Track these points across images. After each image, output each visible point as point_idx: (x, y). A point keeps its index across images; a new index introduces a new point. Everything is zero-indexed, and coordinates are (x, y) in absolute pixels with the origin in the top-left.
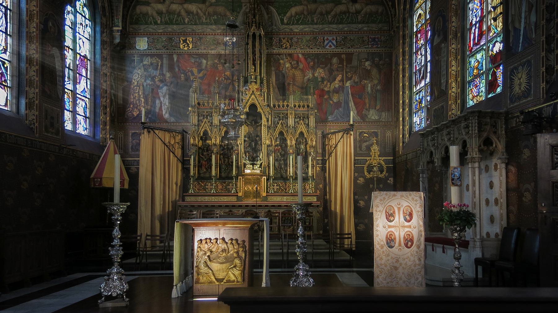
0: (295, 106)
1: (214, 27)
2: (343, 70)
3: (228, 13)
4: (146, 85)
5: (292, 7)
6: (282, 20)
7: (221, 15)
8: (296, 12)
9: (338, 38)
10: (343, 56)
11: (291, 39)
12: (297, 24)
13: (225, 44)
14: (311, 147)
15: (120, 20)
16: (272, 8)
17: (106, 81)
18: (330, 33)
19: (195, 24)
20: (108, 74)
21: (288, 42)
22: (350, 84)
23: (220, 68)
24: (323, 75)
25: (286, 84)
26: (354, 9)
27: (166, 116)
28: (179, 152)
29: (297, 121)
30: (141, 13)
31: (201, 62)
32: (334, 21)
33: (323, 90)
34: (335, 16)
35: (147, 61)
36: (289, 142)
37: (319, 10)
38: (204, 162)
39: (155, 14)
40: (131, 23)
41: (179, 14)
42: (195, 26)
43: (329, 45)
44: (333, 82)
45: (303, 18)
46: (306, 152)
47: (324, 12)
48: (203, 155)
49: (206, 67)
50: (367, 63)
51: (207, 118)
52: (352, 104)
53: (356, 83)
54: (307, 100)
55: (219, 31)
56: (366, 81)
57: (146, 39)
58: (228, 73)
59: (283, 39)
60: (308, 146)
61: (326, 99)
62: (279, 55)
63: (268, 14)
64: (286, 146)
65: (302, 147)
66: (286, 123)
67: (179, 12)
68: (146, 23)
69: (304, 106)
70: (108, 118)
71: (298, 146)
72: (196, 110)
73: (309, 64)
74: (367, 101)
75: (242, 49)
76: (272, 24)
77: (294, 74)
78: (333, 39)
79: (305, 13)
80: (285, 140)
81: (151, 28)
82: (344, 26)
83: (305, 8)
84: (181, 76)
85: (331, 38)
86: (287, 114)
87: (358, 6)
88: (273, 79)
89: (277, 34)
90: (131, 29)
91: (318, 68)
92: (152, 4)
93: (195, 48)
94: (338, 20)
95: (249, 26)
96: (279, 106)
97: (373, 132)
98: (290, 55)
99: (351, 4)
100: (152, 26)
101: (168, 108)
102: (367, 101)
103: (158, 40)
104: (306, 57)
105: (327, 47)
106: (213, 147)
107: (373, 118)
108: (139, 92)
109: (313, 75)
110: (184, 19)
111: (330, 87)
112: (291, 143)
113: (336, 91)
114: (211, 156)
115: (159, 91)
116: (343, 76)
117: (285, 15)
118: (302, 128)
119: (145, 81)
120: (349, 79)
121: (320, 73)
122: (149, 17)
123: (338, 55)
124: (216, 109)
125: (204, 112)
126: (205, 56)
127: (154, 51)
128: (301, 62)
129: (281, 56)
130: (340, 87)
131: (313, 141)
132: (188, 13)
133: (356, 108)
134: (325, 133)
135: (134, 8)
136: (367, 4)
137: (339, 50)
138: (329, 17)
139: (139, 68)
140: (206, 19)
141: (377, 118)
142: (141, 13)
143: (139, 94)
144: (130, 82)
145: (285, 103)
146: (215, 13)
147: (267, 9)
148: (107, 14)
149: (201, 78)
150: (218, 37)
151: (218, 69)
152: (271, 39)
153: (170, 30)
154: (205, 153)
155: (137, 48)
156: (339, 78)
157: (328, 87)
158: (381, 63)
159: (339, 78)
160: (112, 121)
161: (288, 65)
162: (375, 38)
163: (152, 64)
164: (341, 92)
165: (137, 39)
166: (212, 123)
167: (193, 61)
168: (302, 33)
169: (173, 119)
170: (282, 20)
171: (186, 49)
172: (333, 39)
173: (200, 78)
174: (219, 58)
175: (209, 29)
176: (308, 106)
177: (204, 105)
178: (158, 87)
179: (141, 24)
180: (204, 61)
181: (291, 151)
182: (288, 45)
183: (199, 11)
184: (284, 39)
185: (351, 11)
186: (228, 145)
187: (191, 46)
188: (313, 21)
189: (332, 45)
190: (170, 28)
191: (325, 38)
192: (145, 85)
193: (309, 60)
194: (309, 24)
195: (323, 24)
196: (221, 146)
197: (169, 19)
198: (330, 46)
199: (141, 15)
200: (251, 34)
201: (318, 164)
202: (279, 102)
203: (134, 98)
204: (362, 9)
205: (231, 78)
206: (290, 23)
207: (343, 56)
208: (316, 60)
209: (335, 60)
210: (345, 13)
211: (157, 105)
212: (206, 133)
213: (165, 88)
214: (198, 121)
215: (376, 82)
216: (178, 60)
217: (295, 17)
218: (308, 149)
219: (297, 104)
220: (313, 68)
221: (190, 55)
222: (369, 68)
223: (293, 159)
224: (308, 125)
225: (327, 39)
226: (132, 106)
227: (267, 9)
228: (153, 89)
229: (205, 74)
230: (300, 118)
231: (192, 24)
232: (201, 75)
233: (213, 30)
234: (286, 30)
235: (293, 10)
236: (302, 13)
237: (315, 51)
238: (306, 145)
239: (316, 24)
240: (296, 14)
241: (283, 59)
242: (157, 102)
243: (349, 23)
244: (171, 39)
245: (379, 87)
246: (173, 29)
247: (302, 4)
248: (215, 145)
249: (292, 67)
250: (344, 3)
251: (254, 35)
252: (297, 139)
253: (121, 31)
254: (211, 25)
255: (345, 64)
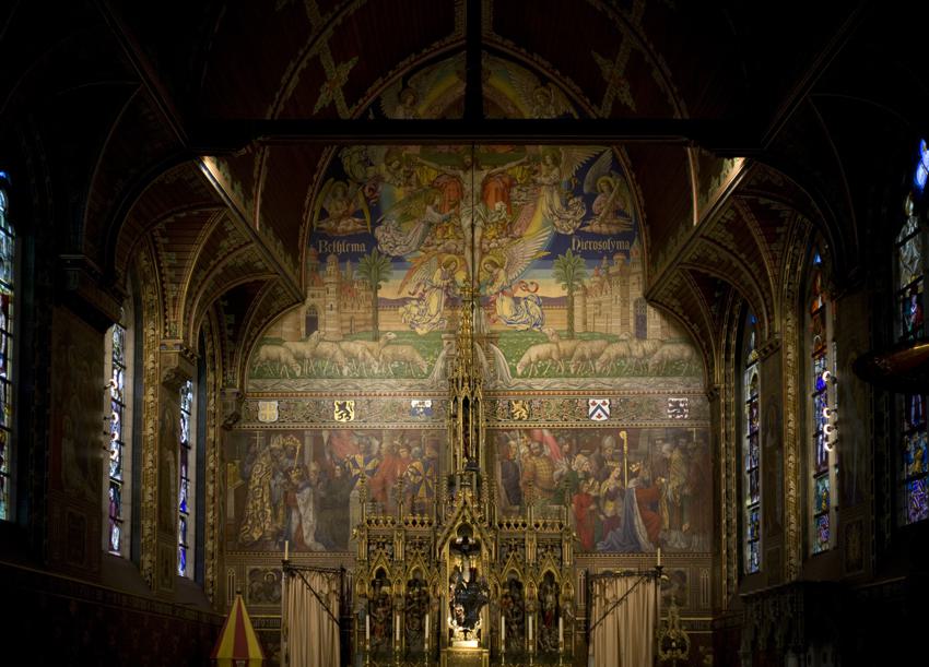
0: (537, 526)
1: (393, 382)
2: (622, 460)
3: (418, 358)
4: (275, 485)
5: (531, 345)
6: (513, 369)
7: (405, 361)
8: (538, 356)
9: (614, 402)
10: (623, 435)
11: (530, 403)
12: (540, 376)
13: (413, 412)
14: (566, 600)
15: (238, 375)
16: (495, 348)
17: (213, 482)
18: (601, 393)
19: (361, 377)
20: (217, 469)
21: (524, 408)
22: (635, 483)
23: (403, 453)
24: (586, 468)
25: (521, 484)
26: (641, 350)
27: (309, 541)
28: (335, 606)
29: (542, 553)
30: (268, 358)
31: (371, 443)
32: (606, 371)
33: (587, 495)
34: (606, 363)
35: (276, 443)
36: (526, 590)
37: (579, 352)
38: (378, 626)
39: (291, 360)
40: (251, 378)
41: (333, 361)
42: (359, 381)
43: (596, 414)
44: (604, 480)
45: (552, 365)
46: (557, 608)
47: (587, 354)
48: (374, 611)
49: (379, 453)
50: (665, 447)
51: (384, 548)
52: (638, 521)
53: (646, 483)
54: (559, 512)
55: (403, 389)
56: (663, 480)
57: (275, 403)
58: (417, 464)
59: (516, 402)
60: (560, 598)
61: (592, 511)
62: (509, 431)
63: (488, 358)
64: (522, 598)
65: (550, 598)
66: (522, 557)
67: (333, 356)
68: (277, 376)
69: (553, 526)
70: (216, 547)
71: (542, 598)
72: (365, 533)
73: (561, 448)
74: (666, 515)
75: (442, 421)
76: (496, 376)
77: (535, 467)
78: (604, 404)
79: (555, 356)
80: (519, 586)
81: (285, 385)
82: (625, 380)
83: (555, 347)
84: (334, 470)
85: (602, 401)
86: (524, 540)
87: (648, 346)
88: (499, 473)
89: (504, 395)
90: (250, 387)
91: (579, 453)
92: (289, 344)
93: (360, 418)
94: (612, 369)
95: (457, 386)
96: (509, 525)
97: (678, 572)
98: (528, 431)
99: (635, 341)
100: (285, 381)
101: (312, 527)
102: (666, 515)
103: (296, 405)
104: (557, 435)
105: (594, 418)
106: (395, 600)
107: (676, 546)
108: (262, 497)
109: (569, 467)
110: (341, 369)
111: (599, 490)
112: (532, 592)
113: (611, 496)
114: (391, 615)
115: (297, 495)
116: (622, 469)
117: (518, 361)
118: (549, 566)
119: (273, 477)
120: (632, 475)
121: (582, 463)
122: (281, 366)
123: (614, 432)
124: (399, 531)
125: (378, 537)
126: (378, 434)
127: (289, 425)
128: (547, 443)
129: (512, 433)
130: (617, 489)
131: (572, 590)
132: (350, 357)
133: (647, 528)
134: (592, 572)
135: (257, 350)
136: (663, 342)
137: (615, 423)
138: (597, 363)
139: (264, 455)
140: (380, 368)
141: (684, 546)
142: (268, 358)
143: (262, 501)
144: (247, 479)
145: (520, 521)
146: (395, 358)
147: (487, 350)
148: (217, 367)
149: (372, 473)
150: (399, 399)
151: (400, 456)
152: (494, 402)
153: (315, 387)
154: (379, 610)
155: (260, 419)
156: (615, 473)
157: (592, 488)
158: (690, 446)
159: (615, 473)
160: (221, 550)
161: (523, 449)
162: (678, 402)
163: (285, 447)
164: (619, 498)
165: (260, 403)
166: (392, 556)
167: (356, 443)
168: (550, 393)
169: (320, 547)
170: (513, 369)
171: (344, 420)
172: (604, 404)
173: (367, 472)
174: (402, 437)
175: (383, 386)
176: (561, 526)
177: (377, 522)
178: (297, 489)
179: (268, 378)
180: (377, 443)
181: (531, 607)
182: (524, 414)
183: (368, 354)
184: (516, 402)
185: (635, 353)
186: (419, 594)
187: (352, 415)
188: (569, 371)
189: (602, 414)
190: (317, 384)
191: (591, 401)
192: (272, 486)
193: (562, 440)
194: (560, 376)
195: (585, 377)
196: (407, 597)
197: (316, 368)
198: (599, 416)
199: (268, 363)
200: (461, 400)
201: (579, 629)
202: (508, 518)
203: (255, 507)
204: (655, 351)
205: (423, 473)
206: (527, 374)
207: (623, 435)
208: (574, 441)
209: (608, 441)
210: (624, 357)
211: (293, 519)
212: (381, 573)
213: (307, 491)
214: (369, 553)
215: (683, 480)
216: (329, 441)
217: (536, 363)
218: (561, 604)
219: (541, 522)
220: (569, 455)
221: (352, 432)
222: (668, 456)
223: (533, 622)
224: (561, 559)
225: (594, 404)
226: (250, 522)
227: (487, 350)
228: (286, 493)
229: (377, 467)
230: (547, 547)
231: (354, 377)
232: (369, 467)
233: (392, 387)
234: (521, 386)
235: (534, 352)
236: (549, 357)
237: (573, 424)
238: (557, 596)
239: (574, 376)
240: (539, 359)
241: (514, 439)
242: (294, 515)
243: (633, 375)
244: (317, 403)
245: (686, 491)
246: (322, 386)
247: (548, 342)
248: (399, 596)
249: (532, 454)
250: (623, 340)
251: (466, 401)
252: (541, 584)
253: (238, 394)
254: (389, 378)
255: (625, 448)
